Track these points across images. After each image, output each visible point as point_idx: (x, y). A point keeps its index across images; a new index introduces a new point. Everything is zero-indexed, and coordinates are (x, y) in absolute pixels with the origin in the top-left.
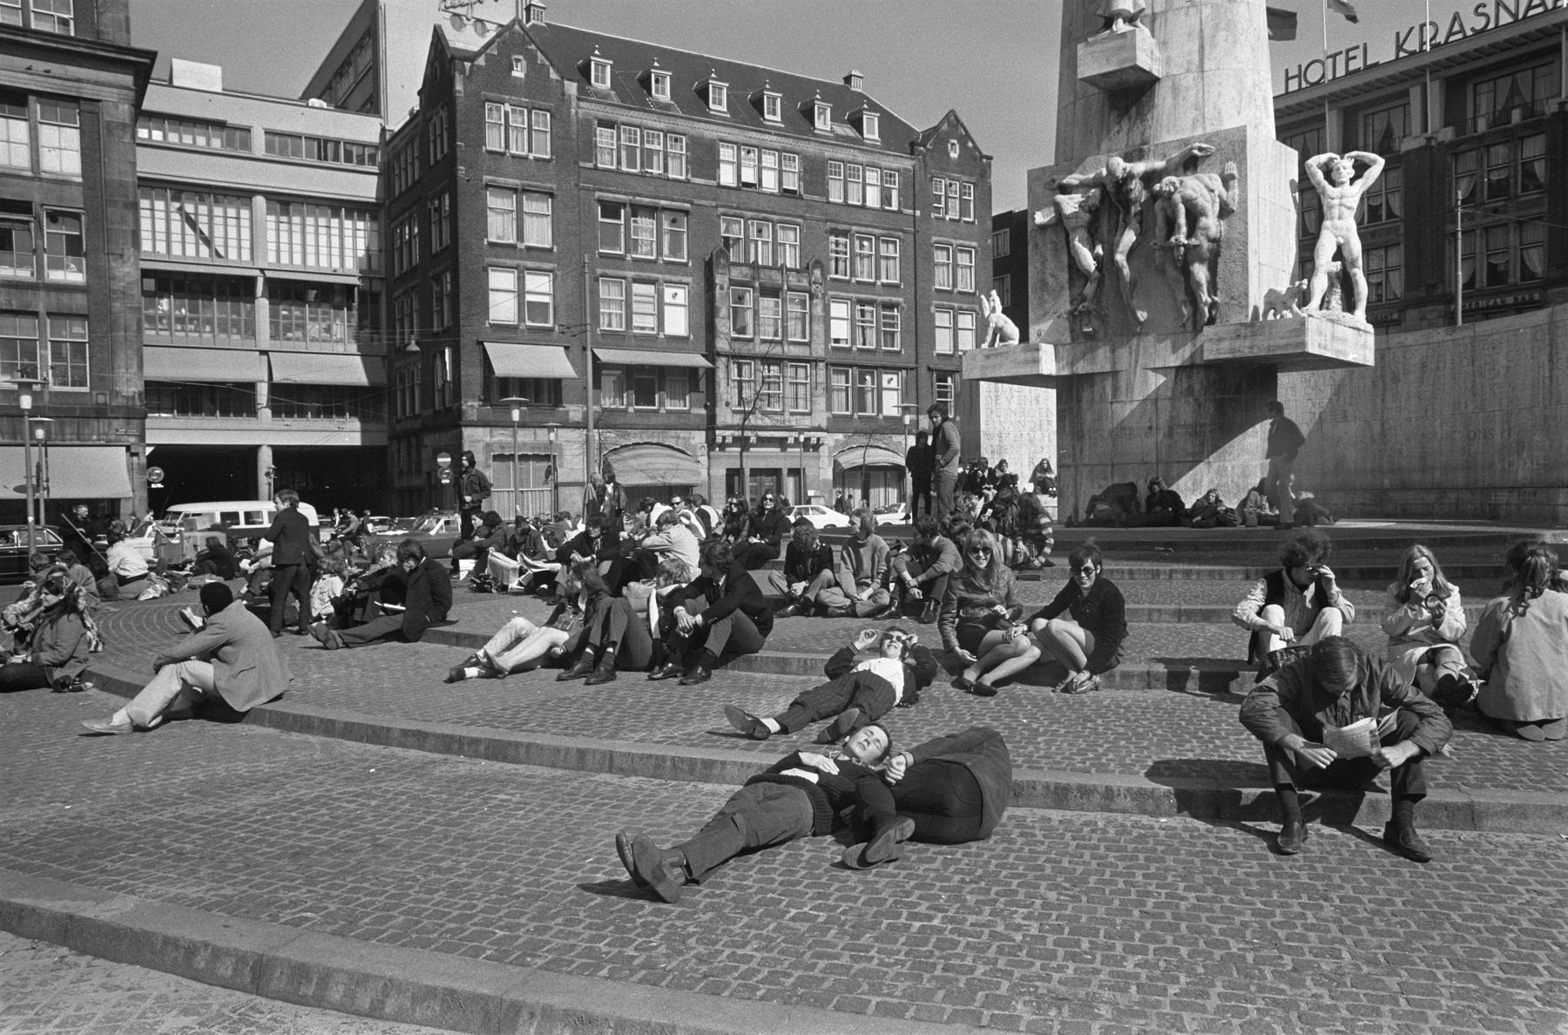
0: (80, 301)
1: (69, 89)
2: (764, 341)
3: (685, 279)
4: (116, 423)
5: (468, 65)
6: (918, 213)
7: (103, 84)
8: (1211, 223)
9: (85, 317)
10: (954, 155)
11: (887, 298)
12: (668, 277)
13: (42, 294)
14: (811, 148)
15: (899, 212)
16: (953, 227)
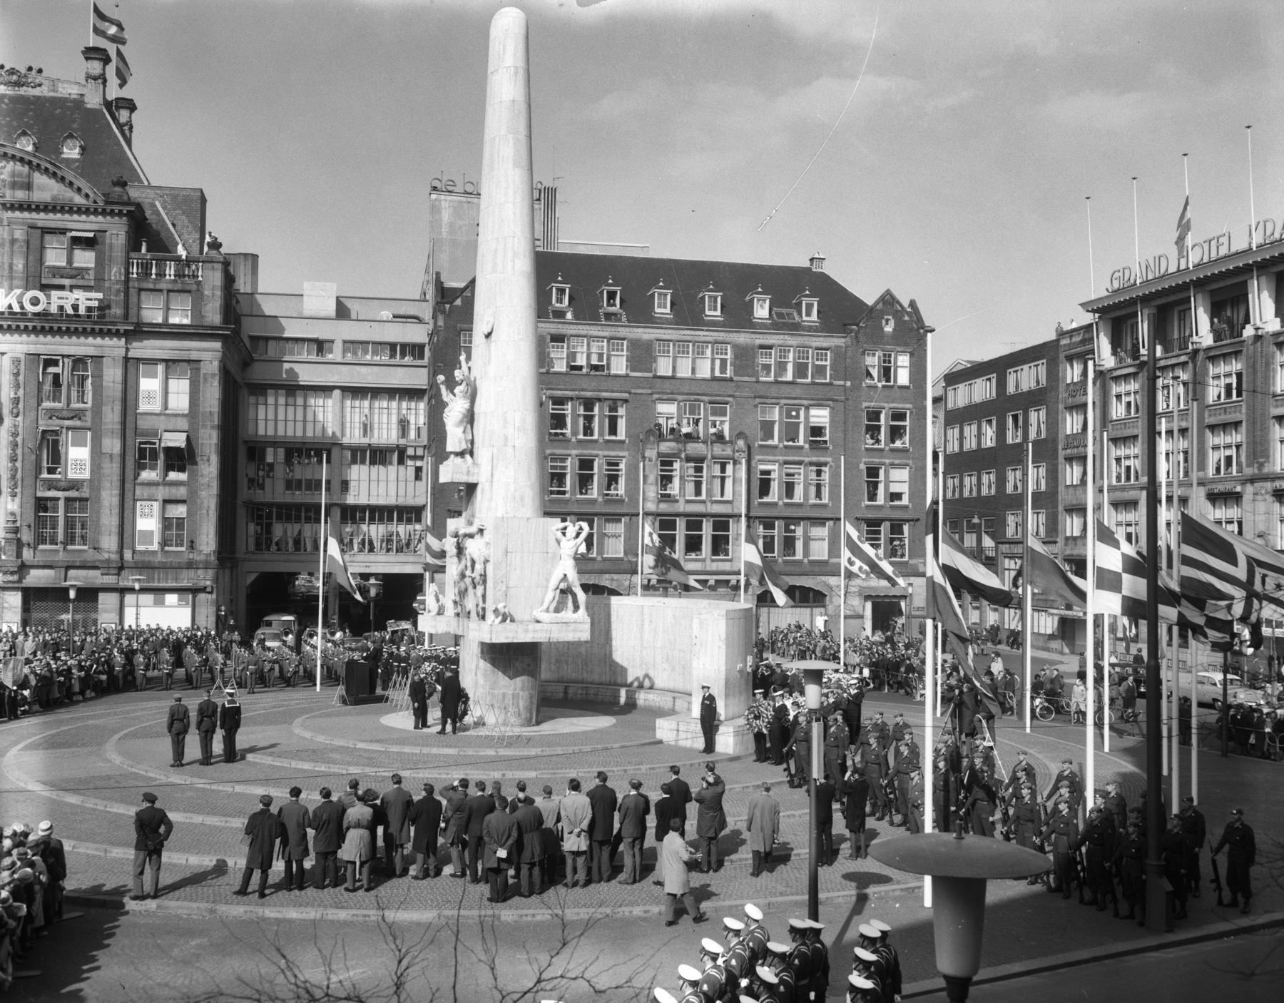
0: (182, 492)
1: (184, 355)
2: (688, 502)
3: (621, 454)
4: (200, 572)
5: (448, 306)
6: (849, 384)
7: (205, 350)
8: (479, 567)
9: (183, 502)
10: (889, 329)
11: (814, 459)
12: (606, 453)
13: (161, 488)
14: (743, 338)
15: (830, 384)
16: (887, 392)
